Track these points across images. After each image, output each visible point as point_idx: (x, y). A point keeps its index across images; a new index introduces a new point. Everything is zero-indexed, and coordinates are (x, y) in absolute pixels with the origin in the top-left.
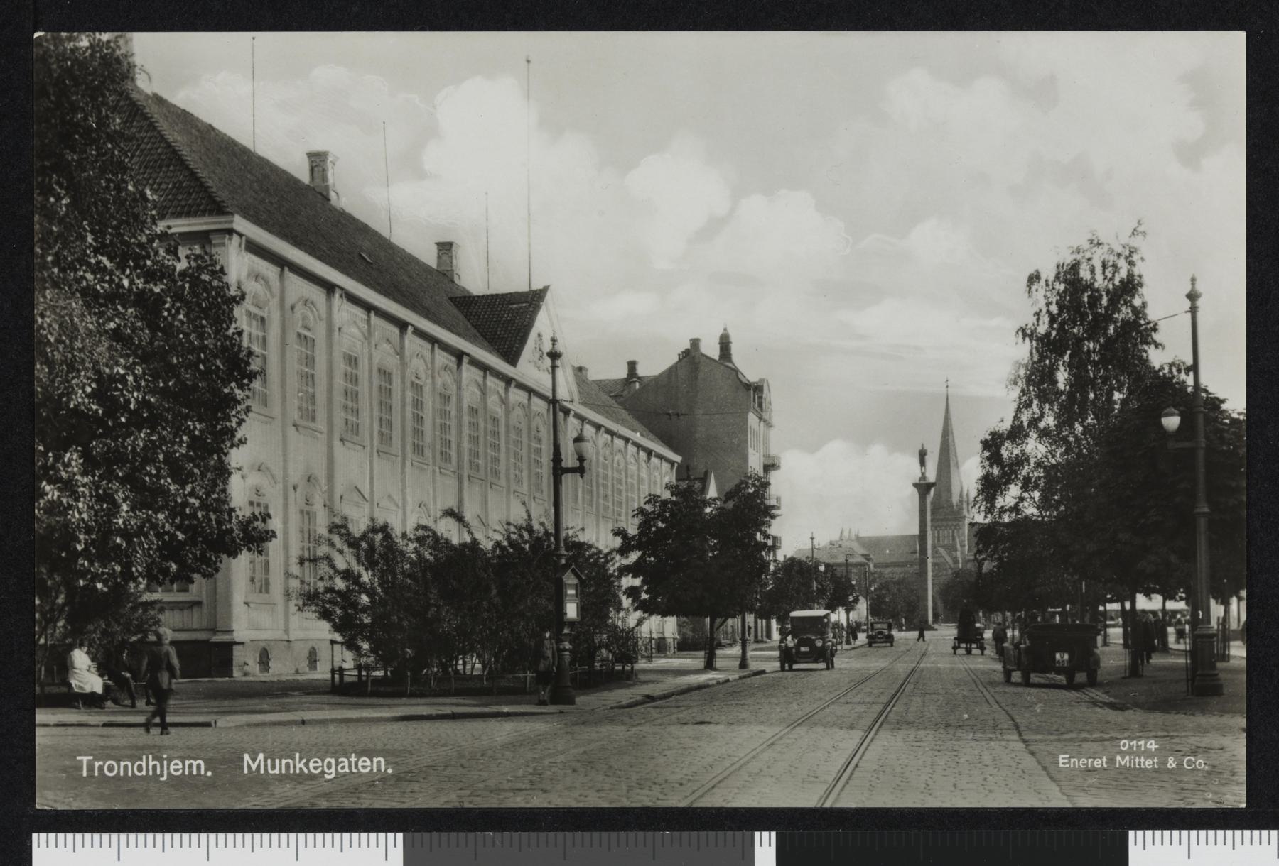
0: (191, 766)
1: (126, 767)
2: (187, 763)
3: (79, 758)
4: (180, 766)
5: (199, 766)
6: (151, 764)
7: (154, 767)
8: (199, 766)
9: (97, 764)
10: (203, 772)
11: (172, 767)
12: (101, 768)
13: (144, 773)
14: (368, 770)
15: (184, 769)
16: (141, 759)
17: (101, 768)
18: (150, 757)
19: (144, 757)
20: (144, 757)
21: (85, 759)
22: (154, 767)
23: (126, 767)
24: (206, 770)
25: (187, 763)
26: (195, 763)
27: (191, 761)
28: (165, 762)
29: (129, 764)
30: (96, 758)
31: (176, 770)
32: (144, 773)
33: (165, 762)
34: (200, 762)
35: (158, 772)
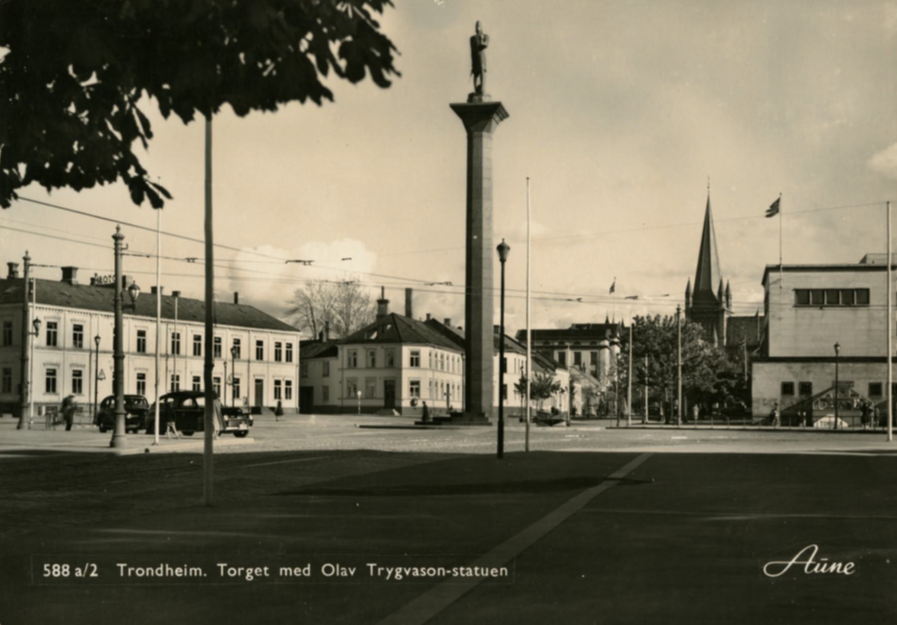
0: (193, 571)
6: (167, 569)
7: (170, 571)
8: (198, 572)
12: (133, 573)
13: (161, 574)
14: (234, 574)
17: (133, 573)
19: (162, 565)
20: (162, 565)
22: (170, 571)
23: (150, 572)
24: (203, 573)
26: (196, 570)
30: (129, 566)
32: (161, 574)
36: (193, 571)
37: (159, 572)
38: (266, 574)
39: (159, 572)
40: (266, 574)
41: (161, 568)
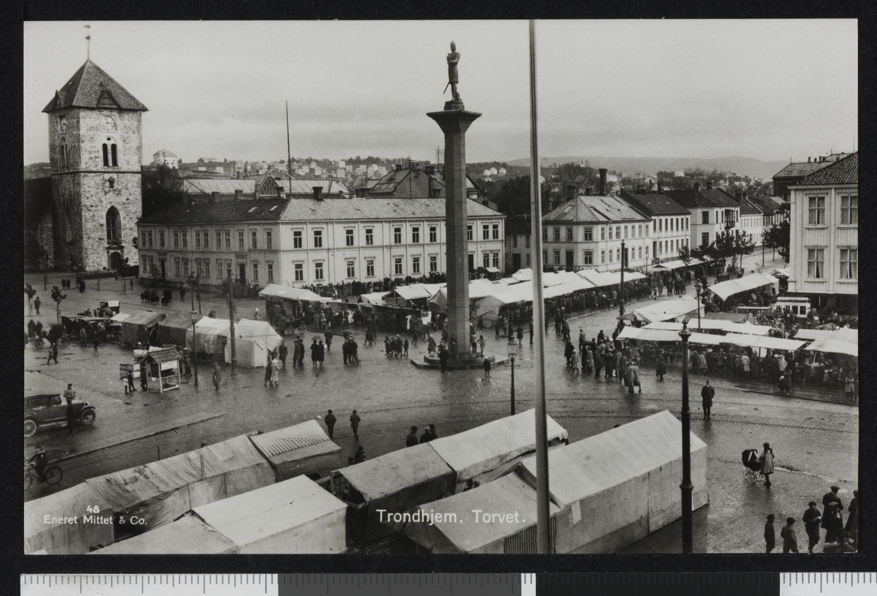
0: (448, 517)
1: (407, 517)
3: (377, 510)
6: (423, 515)
9: (389, 515)
11: (436, 517)
13: (418, 521)
15: (443, 518)
17: (392, 517)
21: (381, 511)
22: (425, 517)
25: (446, 515)
27: (449, 514)
28: (432, 514)
29: (408, 514)
31: (439, 519)
36: (448, 517)
39: (416, 518)
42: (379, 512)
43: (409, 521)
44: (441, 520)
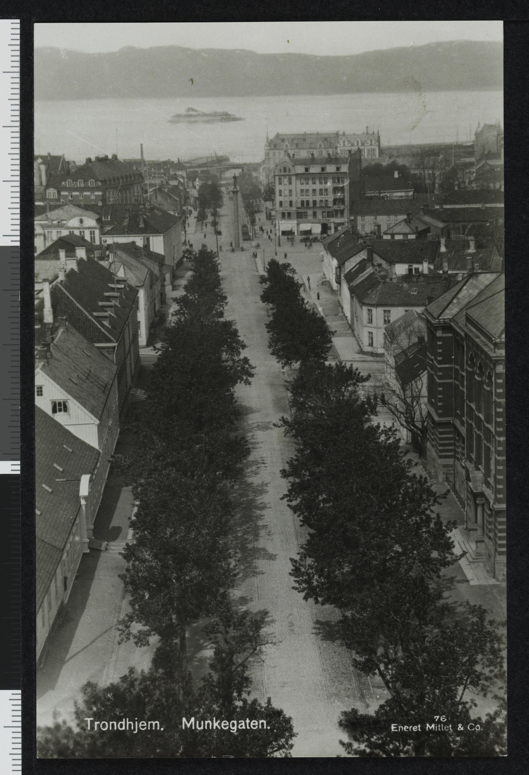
0: (151, 724)
2: (149, 723)
4: (145, 725)
5: (156, 724)
6: (128, 723)
7: (130, 725)
8: (156, 724)
10: (158, 728)
11: (140, 725)
13: (124, 728)
16: (122, 721)
18: (128, 719)
19: (124, 719)
20: (124, 719)
22: (130, 725)
23: (113, 725)
24: (160, 727)
25: (149, 723)
26: (154, 723)
27: (152, 722)
28: (136, 722)
31: (143, 727)
33: (136, 722)
34: (157, 722)
35: (132, 728)
37: (121, 726)
38: (419, 730)
39: (121, 726)
40: (419, 730)
41: (124, 723)
42: (87, 721)
43: (115, 728)
44: (145, 728)
